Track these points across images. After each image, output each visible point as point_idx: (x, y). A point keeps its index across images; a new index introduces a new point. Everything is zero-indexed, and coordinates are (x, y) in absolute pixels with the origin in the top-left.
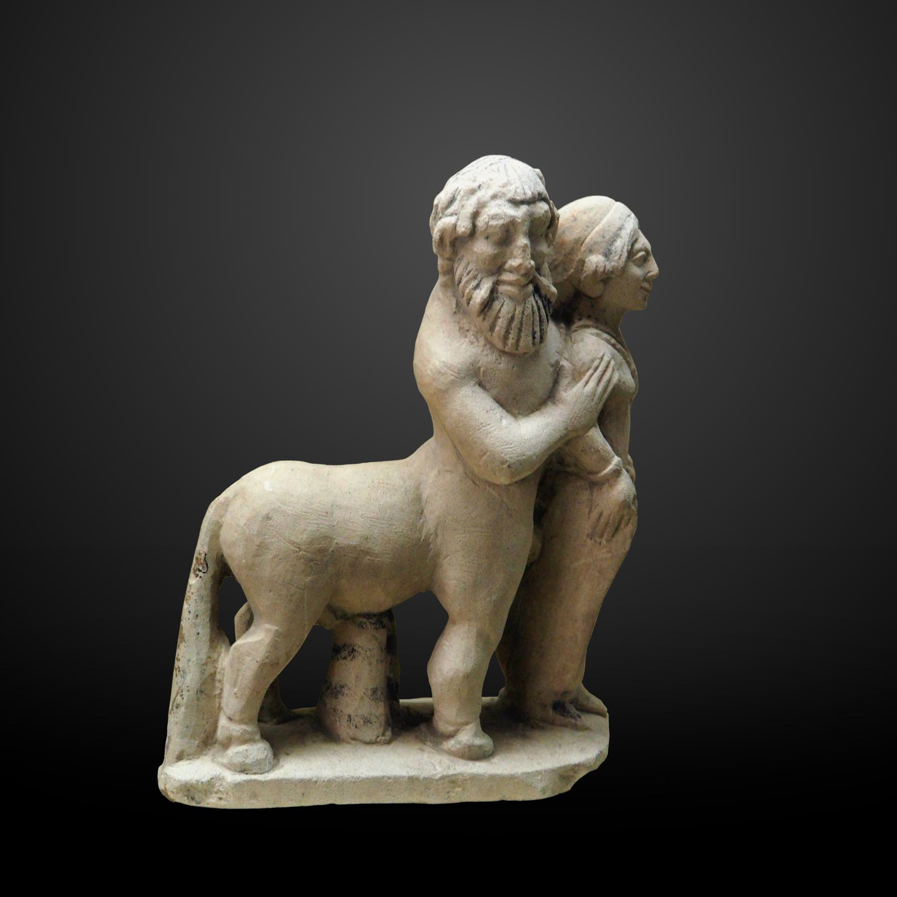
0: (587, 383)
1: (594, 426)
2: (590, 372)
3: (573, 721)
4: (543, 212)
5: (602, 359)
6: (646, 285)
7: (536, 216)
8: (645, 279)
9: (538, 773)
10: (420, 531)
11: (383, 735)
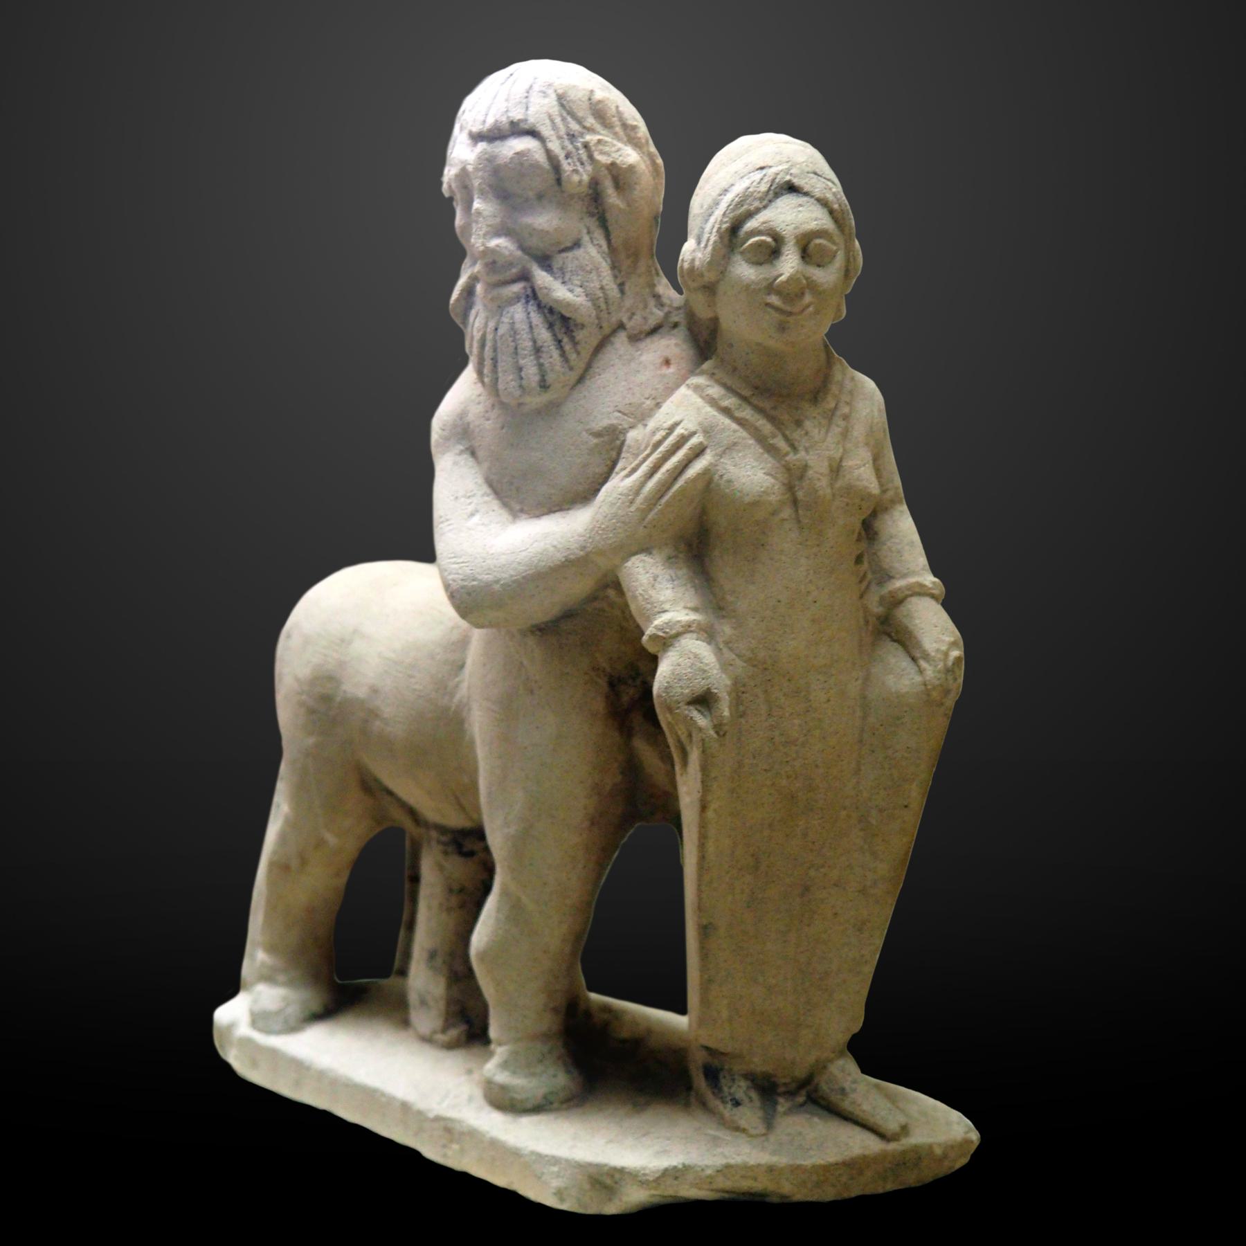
0: (634, 470)
1: (647, 550)
2: (647, 452)
3: (721, 1107)
4: (510, 154)
5: (671, 429)
6: (774, 300)
7: (500, 161)
8: (771, 288)
9: (555, 1160)
10: (452, 695)
11: (444, 1030)
